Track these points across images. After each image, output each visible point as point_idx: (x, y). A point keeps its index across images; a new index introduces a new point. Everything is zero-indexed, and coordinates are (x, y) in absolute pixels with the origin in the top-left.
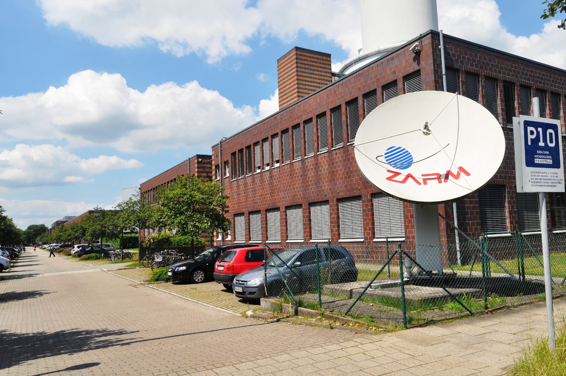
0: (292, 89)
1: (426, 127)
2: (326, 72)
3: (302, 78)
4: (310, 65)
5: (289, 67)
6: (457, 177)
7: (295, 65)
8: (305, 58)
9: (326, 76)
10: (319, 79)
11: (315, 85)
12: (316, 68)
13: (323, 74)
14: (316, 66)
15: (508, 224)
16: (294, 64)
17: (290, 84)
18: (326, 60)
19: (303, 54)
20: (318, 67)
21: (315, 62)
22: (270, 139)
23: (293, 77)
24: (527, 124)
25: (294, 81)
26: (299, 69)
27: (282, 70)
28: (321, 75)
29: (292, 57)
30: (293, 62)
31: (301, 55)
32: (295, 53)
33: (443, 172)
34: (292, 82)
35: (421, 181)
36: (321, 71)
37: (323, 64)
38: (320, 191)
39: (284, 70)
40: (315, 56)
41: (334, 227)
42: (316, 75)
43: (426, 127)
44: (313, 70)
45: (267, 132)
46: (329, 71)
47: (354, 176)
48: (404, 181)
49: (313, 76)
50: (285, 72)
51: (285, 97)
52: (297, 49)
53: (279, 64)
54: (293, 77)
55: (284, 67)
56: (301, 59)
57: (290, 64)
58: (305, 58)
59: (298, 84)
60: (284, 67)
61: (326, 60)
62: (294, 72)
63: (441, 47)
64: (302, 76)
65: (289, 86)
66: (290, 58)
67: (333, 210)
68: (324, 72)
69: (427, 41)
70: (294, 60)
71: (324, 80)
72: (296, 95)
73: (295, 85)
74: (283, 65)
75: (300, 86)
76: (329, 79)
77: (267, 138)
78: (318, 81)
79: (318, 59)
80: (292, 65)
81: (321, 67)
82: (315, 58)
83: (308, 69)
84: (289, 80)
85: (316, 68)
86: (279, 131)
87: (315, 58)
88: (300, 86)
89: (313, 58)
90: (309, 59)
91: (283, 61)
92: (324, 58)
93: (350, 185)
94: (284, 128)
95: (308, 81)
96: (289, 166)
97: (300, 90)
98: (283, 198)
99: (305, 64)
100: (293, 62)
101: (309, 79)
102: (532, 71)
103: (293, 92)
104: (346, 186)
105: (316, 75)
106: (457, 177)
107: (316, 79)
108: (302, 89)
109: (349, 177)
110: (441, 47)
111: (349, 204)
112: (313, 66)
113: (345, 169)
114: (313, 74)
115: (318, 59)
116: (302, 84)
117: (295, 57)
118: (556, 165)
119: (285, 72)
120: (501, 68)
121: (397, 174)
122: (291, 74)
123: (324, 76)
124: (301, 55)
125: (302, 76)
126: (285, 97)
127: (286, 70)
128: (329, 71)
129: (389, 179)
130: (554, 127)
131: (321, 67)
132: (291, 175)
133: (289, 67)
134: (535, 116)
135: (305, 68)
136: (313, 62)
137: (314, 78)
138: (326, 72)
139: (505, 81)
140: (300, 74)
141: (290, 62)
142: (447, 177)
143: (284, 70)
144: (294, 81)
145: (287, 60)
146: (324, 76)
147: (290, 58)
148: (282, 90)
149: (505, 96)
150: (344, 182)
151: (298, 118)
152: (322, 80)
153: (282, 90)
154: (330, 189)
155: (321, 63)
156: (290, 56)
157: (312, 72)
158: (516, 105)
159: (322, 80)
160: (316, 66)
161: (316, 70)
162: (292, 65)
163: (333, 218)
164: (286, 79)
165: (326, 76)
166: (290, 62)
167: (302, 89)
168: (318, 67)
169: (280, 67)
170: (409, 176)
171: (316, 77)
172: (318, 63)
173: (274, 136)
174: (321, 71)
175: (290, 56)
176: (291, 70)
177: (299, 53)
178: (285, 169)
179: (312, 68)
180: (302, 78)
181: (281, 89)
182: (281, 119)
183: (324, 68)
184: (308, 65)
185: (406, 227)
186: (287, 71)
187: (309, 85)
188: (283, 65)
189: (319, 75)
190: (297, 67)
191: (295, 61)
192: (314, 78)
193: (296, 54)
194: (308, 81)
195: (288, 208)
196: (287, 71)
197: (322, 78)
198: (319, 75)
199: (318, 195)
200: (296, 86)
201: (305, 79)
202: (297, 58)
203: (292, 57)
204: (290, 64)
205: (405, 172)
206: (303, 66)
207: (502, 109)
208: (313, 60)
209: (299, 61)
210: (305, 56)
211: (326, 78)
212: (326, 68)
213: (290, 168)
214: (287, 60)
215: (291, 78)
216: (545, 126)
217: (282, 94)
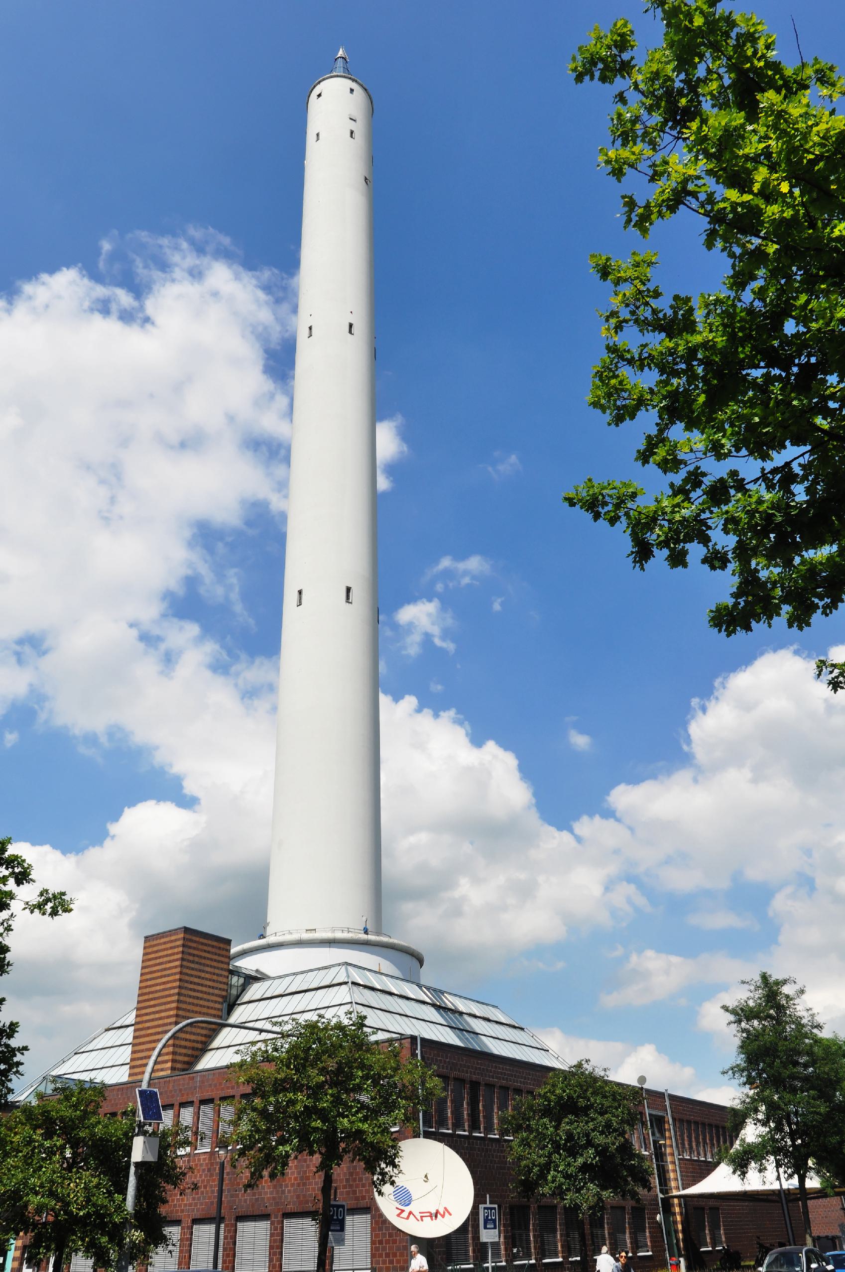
0: (167, 993)
1: (426, 1176)
2: (222, 969)
3: (187, 978)
4: (200, 957)
5: (167, 956)
6: (443, 1216)
7: (180, 956)
8: (194, 945)
9: (221, 975)
10: (210, 980)
11: (204, 989)
12: (208, 962)
13: (217, 971)
14: (208, 959)
15: (471, 1254)
16: (177, 953)
17: (164, 983)
18: (223, 949)
19: (194, 938)
20: (211, 960)
21: (209, 952)
22: (176, 1107)
23: (172, 974)
24: (485, 1208)
25: (175, 981)
26: (185, 963)
27: (153, 956)
28: (214, 974)
29: (176, 940)
30: (176, 950)
31: (191, 941)
32: (182, 935)
33: (434, 1211)
34: (168, 982)
35: (419, 1218)
36: (215, 967)
37: (219, 955)
38: (257, 1200)
39: (156, 958)
40: (210, 942)
41: (275, 1254)
42: (207, 972)
43: (426, 1176)
44: (204, 965)
45: (173, 1097)
46: (225, 966)
47: (310, 1184)
48: (408, 1218)
49: (203, 975)
50: (158, 961)
51: (152, 1003)
52: (187, 930)
53: (148, 944)
54: (172, 974)
55: (157, 952)
56: (190, 947)
57: (170, 952)
58: (194, 945)
59: (180, 987)
60: (157, 952)
61: (223, 949)
62: (176, 967)
63: (418, 1052)
64: (187, 974)
65: (162, 987)
66: (172, 941)
67: (276, 1229)
68: (218, 968)
69: (407, 1043)
70: (178, 946)
71: (217, 981)
72: (174, 1005)
73: (174, 988)
74: (155, 949)
75: (183, 991)
76: (225, 980)
77: (173, 1105)
78: (209, 983)
79: (213, 946)
80: (173, 954)
81: (215, 961)
82: (209, 945)
83: (197, 963)
84: (165, 976)
85: (208, 962)
86: (196, 1098)
87: (209, 945)
88: (183, 991)
89: (206, 945)
90: (200, 947)
91: (155, 942)
92: (222, 945)
93: (304, 1196)
94: (207, 1095)
95: (195, 983)
96: (206, 1156)
97: (182, 998)
98: (190, 1205)
99: (194, 955)
100: (176, 950)
101: (196, 980)
102: (496, 1067)
103: (169, 999)
104: (298, 1197)
105: (207, 972)
106: (443, 1216)
107: (206, 979)
108: (185, 995)
109: (304, 1184)
110: (418, 1052)
111: (300, 1221)
112: (205, 958)
113: (299, 1173)
114: (203, 971)
115: (213, 946)
116: (186, 988)
117: (180, 943)
118: (495, 1228)
119: (158, 961)
120: (468, 1067)
121: (403, 1211)
122: (170, 968)
123: (218, 975)
124: (191, 941)
125: (187, 974)
126: (152, 1003)
127: (160, 957)
128: (225, 966)
129: (398, 1215)
130: (495, 1209)
131: (215, 961)
132: (209, 1170)
133: (167, 956)
134: (488, 1205)
135: (193, 962)
136: (205, 951)
137: (203, 978)
138: (222, 969)
139: (471, 1082)
140: (185, 970)
141: (171, 948)
142: (436, 1217)
143: (156, 958)
144: (175, 981)
145: (165, 943)
146: (218, 975)
147: (172, 941)
148: (147, 990)
149: (471, 1099)
150: (295, 1191)
151: (233, 1088)
152: (214, 981)
153: (147, 990)
154: (274, 1198)
155: (216, 954)
156: (173, 938)
157: (202, 967)
158: (481, 1108)
159: (214, 981)
160: (208, 959)
161: (208, 966)
162: (173, 954)
163: (275, 1241)
164: (159, 974)
165: (221, 975)
166: (171, 948)
167: (185, 995)
168: (211, 960)
169: (150, 950)
170: (410, 1213)
171: (207, 976)
172: (212, 953)
173: (183, 1105)
174: (215, 967)
175: (173, 938)
176: (170, 962)
177: (188, 936)
178: (199, 1160)
179: (203, 961)
180: (187, 978)
181: (146, 987)
182: (202, 1082)
183: (219, 961)
184: (198, 956)
185: (373, 1256)
186: (161, 960)
187: (194, 990)
188: (155, 949)
189: (211, 973)
190: (182, 959)
191: (181, 949)
192: (203, 978)
193: (184, 938)
194: (195, 983)
195: (196, 1221)
196: (161, 960)
197: (215, 977)
198: (211, 973)
199: (253, 1205)
200: (176, 991)
201: (192, 979)
202: (183, 946)
203: (176, 940)
204: (170, 952)
205: (407, 1209)
206: (191, 958)
207: (468, 1114)
208: (205, 948)
209: (186, 950)
210: (195, 942)
211: (220, 979)
212: (222, 962)
213: (210, 1159)
214: (165, 943)
215: (168, 975)
216: (491, 1209)
217: (146, 997)
